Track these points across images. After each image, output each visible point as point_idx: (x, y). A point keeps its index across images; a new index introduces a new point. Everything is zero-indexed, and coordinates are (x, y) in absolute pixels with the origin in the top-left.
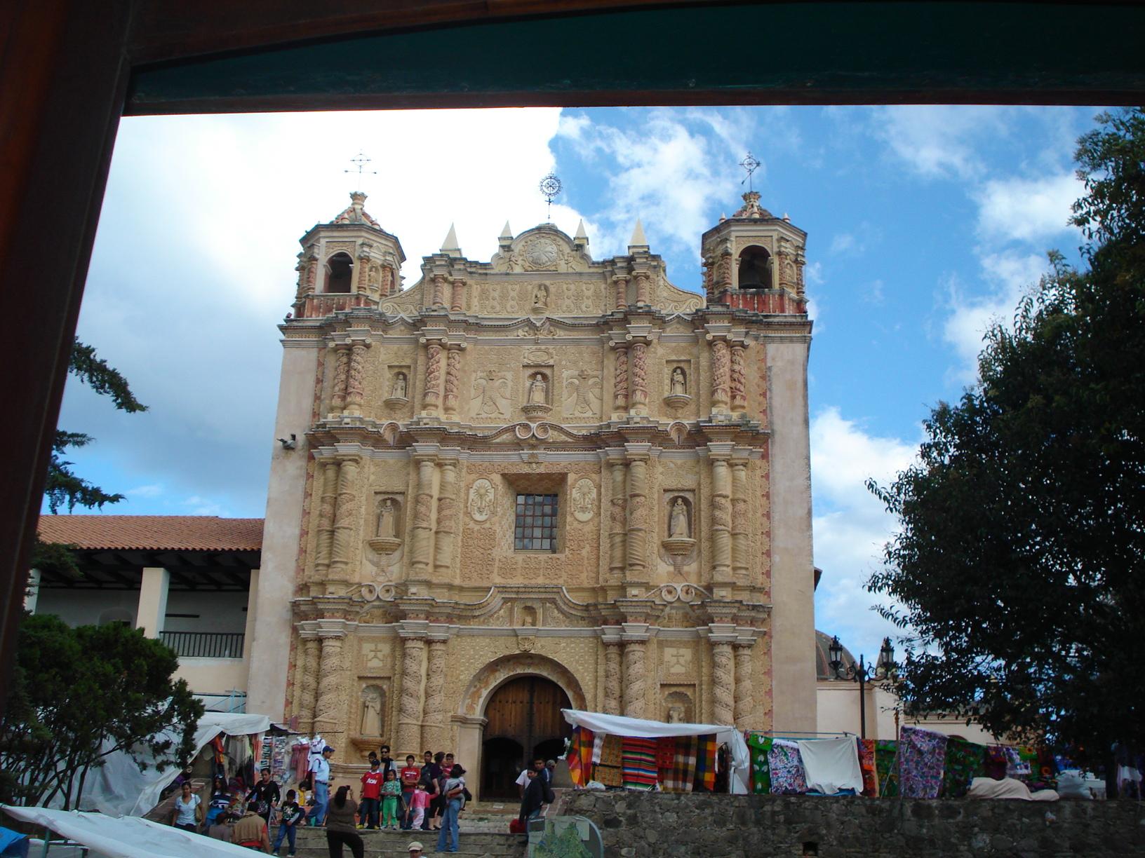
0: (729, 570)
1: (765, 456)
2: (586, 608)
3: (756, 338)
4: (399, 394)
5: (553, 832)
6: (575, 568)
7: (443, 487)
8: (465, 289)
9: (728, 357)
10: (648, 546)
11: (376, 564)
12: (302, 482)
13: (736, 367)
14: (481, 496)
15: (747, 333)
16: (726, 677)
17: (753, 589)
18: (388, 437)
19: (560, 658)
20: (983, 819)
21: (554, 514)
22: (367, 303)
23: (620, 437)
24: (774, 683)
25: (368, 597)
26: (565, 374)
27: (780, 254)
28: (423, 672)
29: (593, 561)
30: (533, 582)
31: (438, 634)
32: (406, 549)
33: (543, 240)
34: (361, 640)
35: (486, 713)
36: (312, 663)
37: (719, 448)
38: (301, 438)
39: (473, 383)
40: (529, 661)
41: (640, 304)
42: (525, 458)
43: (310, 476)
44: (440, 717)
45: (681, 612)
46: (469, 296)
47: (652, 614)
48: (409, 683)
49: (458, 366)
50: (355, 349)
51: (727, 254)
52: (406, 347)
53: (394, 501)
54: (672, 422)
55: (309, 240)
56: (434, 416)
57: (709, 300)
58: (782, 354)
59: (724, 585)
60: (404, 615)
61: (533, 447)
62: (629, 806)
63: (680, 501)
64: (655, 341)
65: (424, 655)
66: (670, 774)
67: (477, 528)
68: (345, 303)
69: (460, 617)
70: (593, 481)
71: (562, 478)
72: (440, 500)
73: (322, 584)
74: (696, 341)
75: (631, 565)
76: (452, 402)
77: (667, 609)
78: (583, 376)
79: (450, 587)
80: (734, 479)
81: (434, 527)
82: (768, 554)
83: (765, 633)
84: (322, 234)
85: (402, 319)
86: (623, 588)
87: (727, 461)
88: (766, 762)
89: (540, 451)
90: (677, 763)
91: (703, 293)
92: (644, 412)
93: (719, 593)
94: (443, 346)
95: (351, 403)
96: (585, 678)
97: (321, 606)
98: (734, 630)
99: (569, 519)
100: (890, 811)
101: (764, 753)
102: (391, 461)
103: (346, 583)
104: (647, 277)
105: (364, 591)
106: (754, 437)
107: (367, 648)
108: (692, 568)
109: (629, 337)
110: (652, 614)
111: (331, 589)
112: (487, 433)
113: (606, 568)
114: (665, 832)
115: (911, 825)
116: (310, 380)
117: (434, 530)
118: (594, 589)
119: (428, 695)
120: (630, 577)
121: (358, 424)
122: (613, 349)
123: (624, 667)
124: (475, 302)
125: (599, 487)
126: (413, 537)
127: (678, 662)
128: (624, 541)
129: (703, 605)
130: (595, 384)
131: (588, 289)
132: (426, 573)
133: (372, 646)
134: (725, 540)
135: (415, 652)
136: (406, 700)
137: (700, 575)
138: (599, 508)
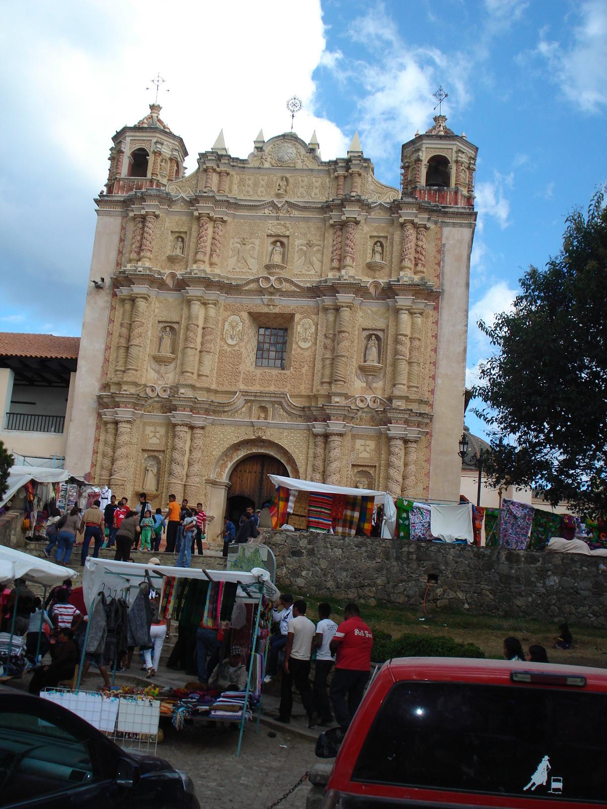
0: (405, 387)
1: (436, 308)
2: (303, 409)
3: (436, 223)
4: (178, 252)
5: (244, 554)
6: (297, 381)
7: (206, 319)
9: (414, 235)
10: (349, 368)
11: (158, 372)
12: (108, 312)
13: (420, 243)
14: (233, 328)
15: (429, 219)
16: (398, 462)
17: (421, 402)
18: (170, 282)
19: (283, 443)
20: (556, 566)
21: (284, 343)
22: (157, 185)
23: (333, 289)
25: (151, 394)
26: (297, 242)
27: (457, 162)
28: (187, 448)
30: (267, 389)
31: (198, 422)
32: (179, 362)
33: (286, 144)
34: (145, 424)
35: (230, 479)
36: (110, 438)
37: (403, 301)
38: (108, 281)
40: (262, 444)
41: (353, 194)
42: (266, 301)
43: (113, 308)
44: (197, 480)
46: (231, 183)
47: (349, 415)
48: (177, 455)
49: (220, 233)
51: (419, 160)
52: (184, 218)
53: (172, 328)
54: (371, 280)
55: (118, 138)
56: (202, 269)
57: (404, 194)
58: (453, 235)
59: (400, 398)
60: (175, 408)
61: (271, 294)
62: (309, 543)
63: (373, 337)
64: (363, 221)
65: (188, 437)
66: (341, 522)
67: (229, 349)
68: (142, 185)
69: (215, 412)
71: (291, 317)
72: (204, 328)
73: (119, 384)
74: (392, 222)
75: (336, 381)
76: (215, 259)
77: (360, 413)
78: (309, 245)
79: (209, 390)
80: (413, 324)
81: (199, 347)
82: (433, 378)
83: (427, 433)
84: (128, 134)
86: (329, 397)
87: (408, 310)
88: (408, 518)
89: (276, 297)
90: (346, 515)
91: (400, 188)
92: (351, 272)
93: (396, 403)
94: (211, 219)
95: (144, 257)
96: (300, 459)
97: (117, 400)
98: (406, 430)
99: (294, 346)
100: (490, 557)
101: (407, 512)
103: (136, 384)
104: (360, 175)
105: (148, 390)
106: (429, 294)
107: (149, 430)
108: (379, 385)
109: (344, 218)
110: (349, 415)
111: (125, 387)
112: (239, 282)
113: (319, 382)
114: (333, 562)
115: (503, 567)
117: (199, 348)
118: (309, 396)
119: (190, 464)
120: (334, 389)
121: (148, 272)
122: (332, 226)
123: (327, 451)
124: (235, 187)
126: (184, 354)
127: (365, 450)
128: (332, 364)
129: (384, 411)
130: (318, 251)
131: (317, 181)
132: (192, 379)
133: (152, 429)
134: (403, 366)
135: (182, 434)
136: (174, 466)
138: (316, 339)
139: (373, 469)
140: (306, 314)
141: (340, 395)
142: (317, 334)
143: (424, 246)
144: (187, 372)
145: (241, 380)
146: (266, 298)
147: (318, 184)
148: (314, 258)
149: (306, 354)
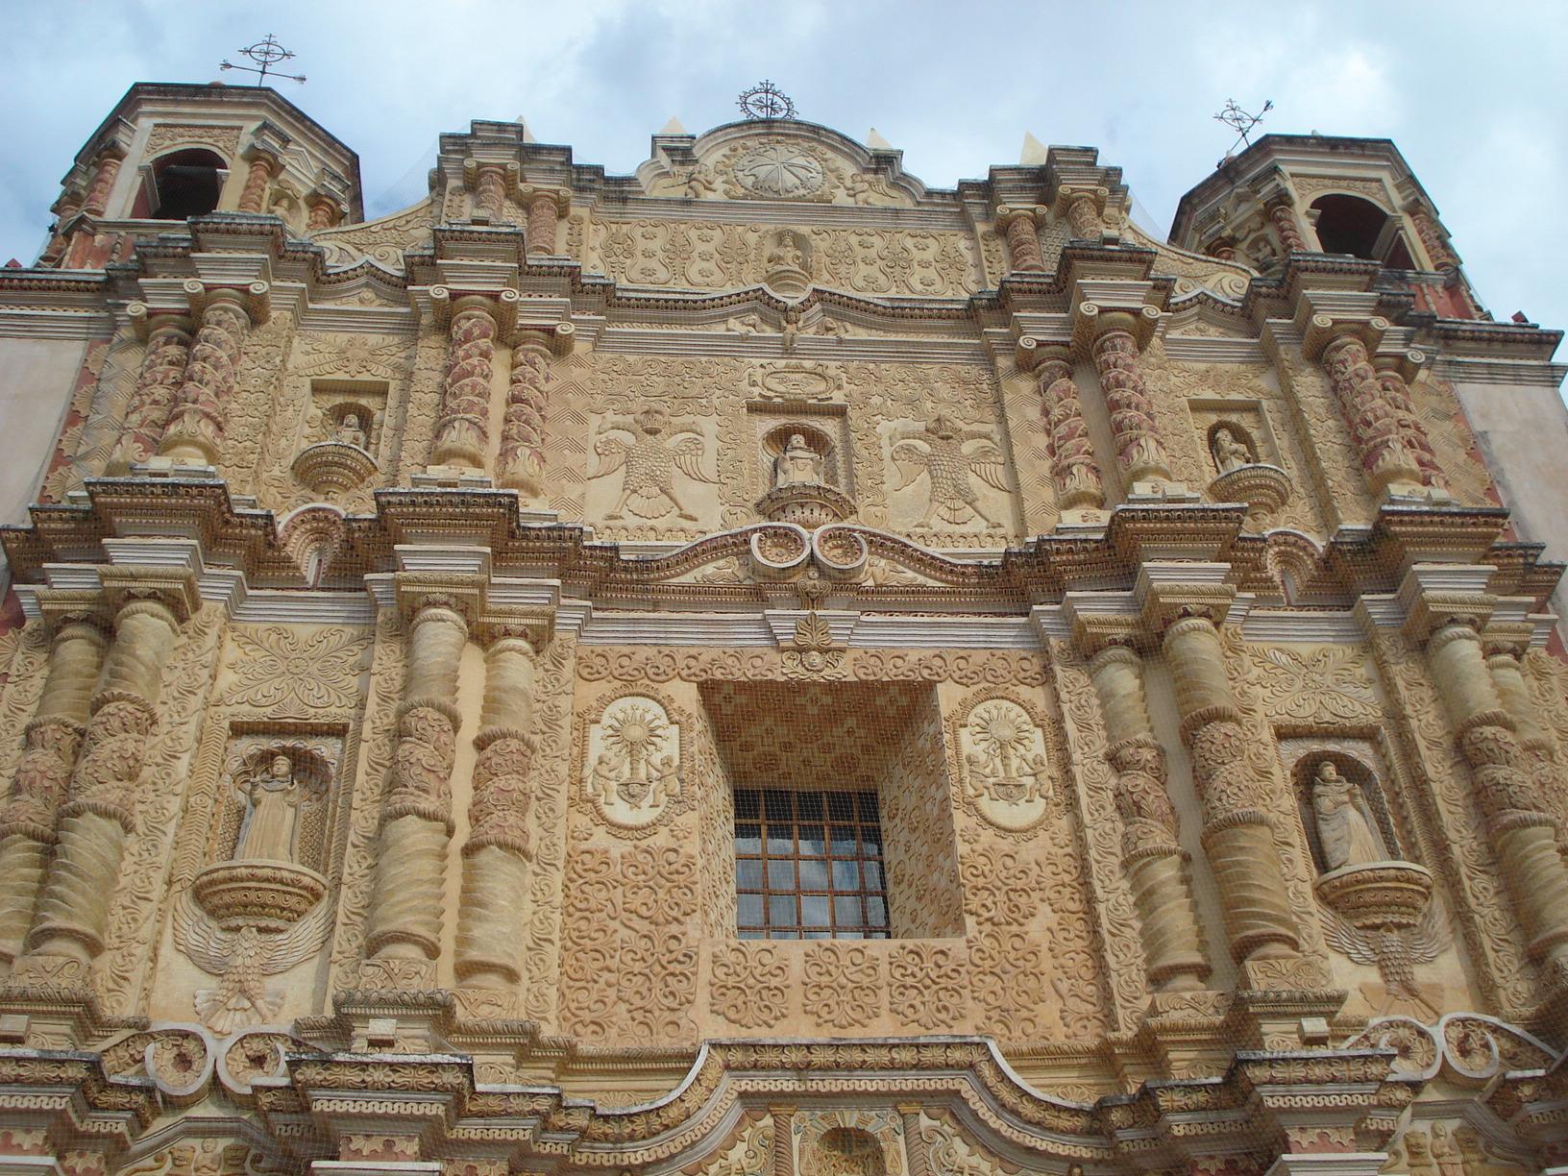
7: (492, 705)
8: (563, 227)
11: (215, 968)
14: (633, 748)
18: (309, 563)
23: (1115, 556)
25: (171, 1081)
26: (884, 427)
29: (1079, 963)
30: (855, 1034)
33: (778, 147)
39: (594, 439)
45: (1450, 1125)
46: (575, 243)
50: (209, 315)
52: (374, 339)
53: (306, 767)
61: (810, 599)
63: (1330, 770)
67: (618, 848)
76: (525, 465)
78: (940, 432)
79: (526, 1045)
80: (1503, 693)
84: (146, 108)
85: (374, 273)
86: (1239, 1022)
87: (1478, 624)
99: (960, 820)
103: (86, 1016)
109: (1089, 308)
113: (1140, 980)
116: (49, 417)
117: (462, 837)
120: (1261, 978)
137: (1484, 990)
138: (1068, 782)
142: (1065, 765)
145: (703, 997)
146: (785, 618)
147: (932, 253)
148: (972, 479)
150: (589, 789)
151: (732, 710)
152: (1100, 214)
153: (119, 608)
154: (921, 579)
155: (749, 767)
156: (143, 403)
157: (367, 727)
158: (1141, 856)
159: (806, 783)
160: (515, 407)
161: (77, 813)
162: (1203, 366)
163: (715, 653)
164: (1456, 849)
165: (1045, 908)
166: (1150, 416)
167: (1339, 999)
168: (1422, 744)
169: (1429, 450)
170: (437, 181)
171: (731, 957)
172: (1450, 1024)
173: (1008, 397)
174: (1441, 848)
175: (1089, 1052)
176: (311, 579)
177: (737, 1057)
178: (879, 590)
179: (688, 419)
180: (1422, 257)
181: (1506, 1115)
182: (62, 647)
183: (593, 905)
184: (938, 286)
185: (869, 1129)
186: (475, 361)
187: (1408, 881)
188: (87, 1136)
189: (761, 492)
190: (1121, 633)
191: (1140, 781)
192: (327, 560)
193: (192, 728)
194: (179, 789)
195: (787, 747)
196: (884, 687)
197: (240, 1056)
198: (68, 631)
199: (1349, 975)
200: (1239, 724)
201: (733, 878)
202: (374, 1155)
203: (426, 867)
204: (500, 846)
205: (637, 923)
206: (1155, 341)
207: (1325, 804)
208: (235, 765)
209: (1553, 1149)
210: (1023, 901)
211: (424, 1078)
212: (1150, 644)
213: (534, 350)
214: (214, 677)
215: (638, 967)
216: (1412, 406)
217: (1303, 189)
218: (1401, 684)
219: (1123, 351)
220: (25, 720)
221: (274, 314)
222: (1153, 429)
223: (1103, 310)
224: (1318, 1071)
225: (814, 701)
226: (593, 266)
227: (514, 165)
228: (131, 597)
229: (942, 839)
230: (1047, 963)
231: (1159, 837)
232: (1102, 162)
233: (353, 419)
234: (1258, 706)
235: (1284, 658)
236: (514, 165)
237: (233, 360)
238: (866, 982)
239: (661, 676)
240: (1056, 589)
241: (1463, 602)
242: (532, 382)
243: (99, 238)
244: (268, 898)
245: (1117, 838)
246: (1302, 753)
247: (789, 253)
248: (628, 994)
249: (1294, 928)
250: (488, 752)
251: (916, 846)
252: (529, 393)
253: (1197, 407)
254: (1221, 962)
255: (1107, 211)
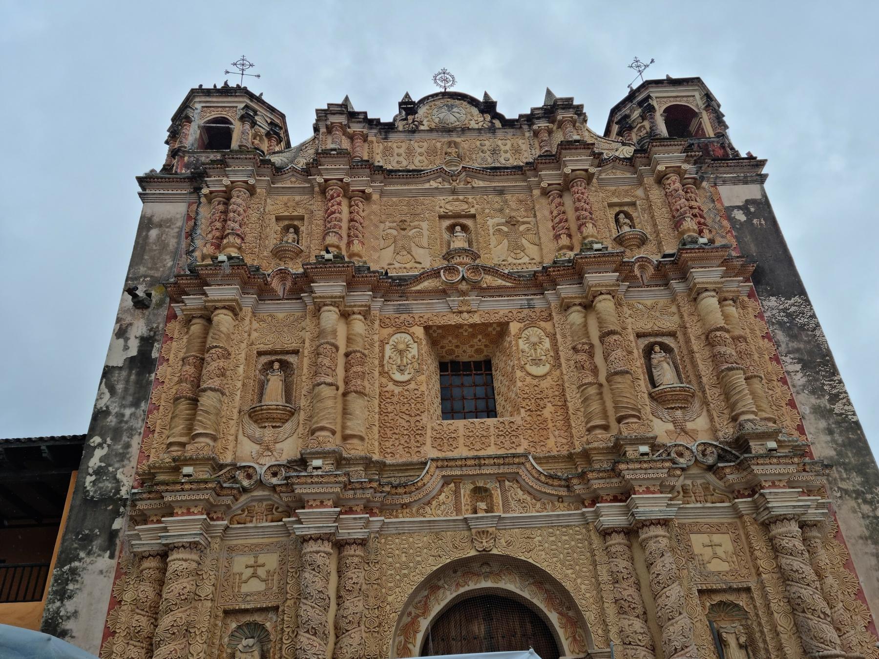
7: (349, 340)
11: (258, 442)
13: (693, 203)
14: (401, 352)
23: (575, 271)
24: (861, 579)
26: (491, 222)
28: (332, 592)
36: (147, 590)
39: (382, 233)
46: (371, 152)
48: (308, 611)
50: (234, 193)
52: (297, 198)
53: (285, 366)
61: (463, 293)
63: (657, 348)
67: (397, 390)
69: (383, 509)
70: (544, 330)
71: (503, 327)
76: (356, 247)
78: (512, 223)
79: (368, 463)
80: (726, 317)
84: (197, 99)
97: (168, 498)
99: (519, 374)
102: (281, 316)
105: (240, 475)
108: (699, 424)
113: (583, 430)
117: (341, 390)
119: (339, 632)
125: (553, 337)
135: (319, 560)
137: (714, 431)
138: (557, 357)
139: (744, 595)
140: (531, 323)
141: (643, 441)
142: (557, 352)
143: (702, 208)
144: (322, 429)
145: (429, 441)
147: (508, 147)
148: (524, 241)
149: (544, 384)
150: (386, 369)
151: (435, 335)
152: (574, 126)
153: (212, 313)
154: (504, 283)
155: (444, 354)
156: (212, 230)
157: (306, 352)
158: (583, 385)
159: (465, 358)
160: (353, 223)
161: (204, 390)
162: (614, 188)
163: (429, 315)
164: (705, 380)
165: (549, 405)
166: (590, 213)
167: (655, 438)
168: (693, 338)
169: (704, 218)
170: (316, 129)
171: (437, 428)
172: (699, 445)
173: (537, 207)
174: (699, 377)
175: (564, 456)
176: (281, 294)
177: (440, 464)
178: (489, 288)
179: (416, 223)
180: (710, 131)
181: (721, 479)
182: (192, 328)
183: (389, 410)
184: (511, 161)
185: (488, 486)
186: (335, 207)
187: (685, 391)
188: (217, 505)
189: (444, 252)
190: (578, 301)
191: (584, 357)
192: (287, 288)
193: (243, 355)
194: (240, 378)
195: (457, 347)
196: (491, 324)
197: (269, 473)
198: (194, 321)
199: (661, 428)
200: (620, 335)
201: (439, 395)
202: (317, 506)
203: (330, 403)
204: (356, 392)
205: (405, 416)
206: (594, 180)
207: (654, 362)
208: (260, 367)
209: (739, 491)
210: (541, 403)
211: (332, 479)
212: (588, 307)
213: (357, 200)
214: (249, 335)
215: (405, 432)
216: (698, 199)
217: (661, 102)
218: (685, 315)
219: (579, 187)
220: (181, 355)
221: (258, 190)
222: (591, 219)
223: (573, 171)
224: (645, 465)
225: (466, 331)
226: (379, 161)
227: (345, 122)
228: (216, 308)
229: (513, 381)
230: (550, 425)
231: (590, 379)
232: (575, 103)
233: (292, 230)
234: (629, 327)
235: (640, 306)
236: (345, 122)
237: (245, 211)
238: (485, 434)
239: (411, 325)
240: (554, 284)
241: (711, 283)
242: (358, 213)
243: (186, 158)
244: (275, 416)
245: (575, 378)
246: (646, 342)
247: (453, 150)
248: (403, 442)
249: (640, 412)
250: (350, 358)
251: (504, 382)
252: (357, 218)
253: (611, 205)
254: (613, 424)
255: (577, 124)
